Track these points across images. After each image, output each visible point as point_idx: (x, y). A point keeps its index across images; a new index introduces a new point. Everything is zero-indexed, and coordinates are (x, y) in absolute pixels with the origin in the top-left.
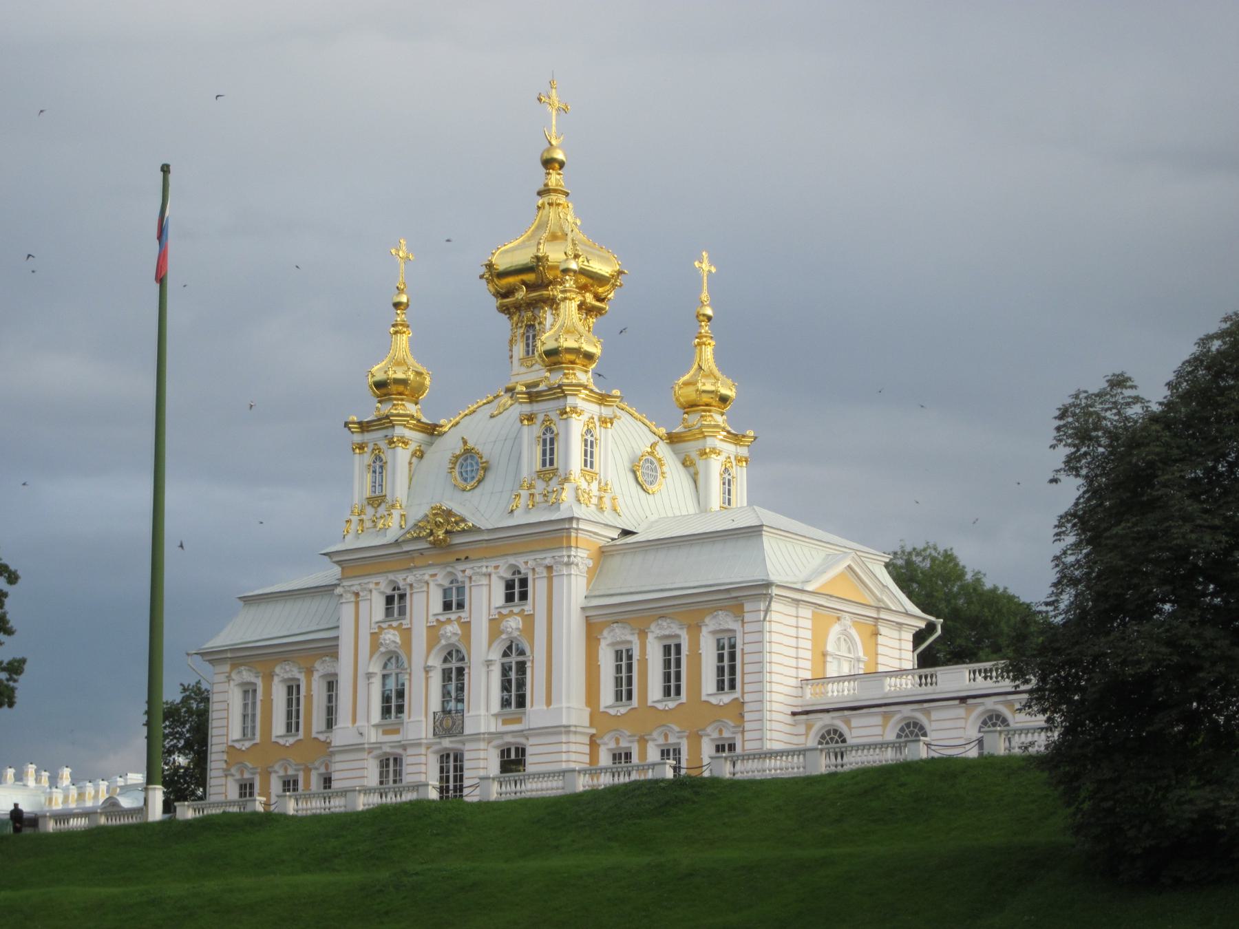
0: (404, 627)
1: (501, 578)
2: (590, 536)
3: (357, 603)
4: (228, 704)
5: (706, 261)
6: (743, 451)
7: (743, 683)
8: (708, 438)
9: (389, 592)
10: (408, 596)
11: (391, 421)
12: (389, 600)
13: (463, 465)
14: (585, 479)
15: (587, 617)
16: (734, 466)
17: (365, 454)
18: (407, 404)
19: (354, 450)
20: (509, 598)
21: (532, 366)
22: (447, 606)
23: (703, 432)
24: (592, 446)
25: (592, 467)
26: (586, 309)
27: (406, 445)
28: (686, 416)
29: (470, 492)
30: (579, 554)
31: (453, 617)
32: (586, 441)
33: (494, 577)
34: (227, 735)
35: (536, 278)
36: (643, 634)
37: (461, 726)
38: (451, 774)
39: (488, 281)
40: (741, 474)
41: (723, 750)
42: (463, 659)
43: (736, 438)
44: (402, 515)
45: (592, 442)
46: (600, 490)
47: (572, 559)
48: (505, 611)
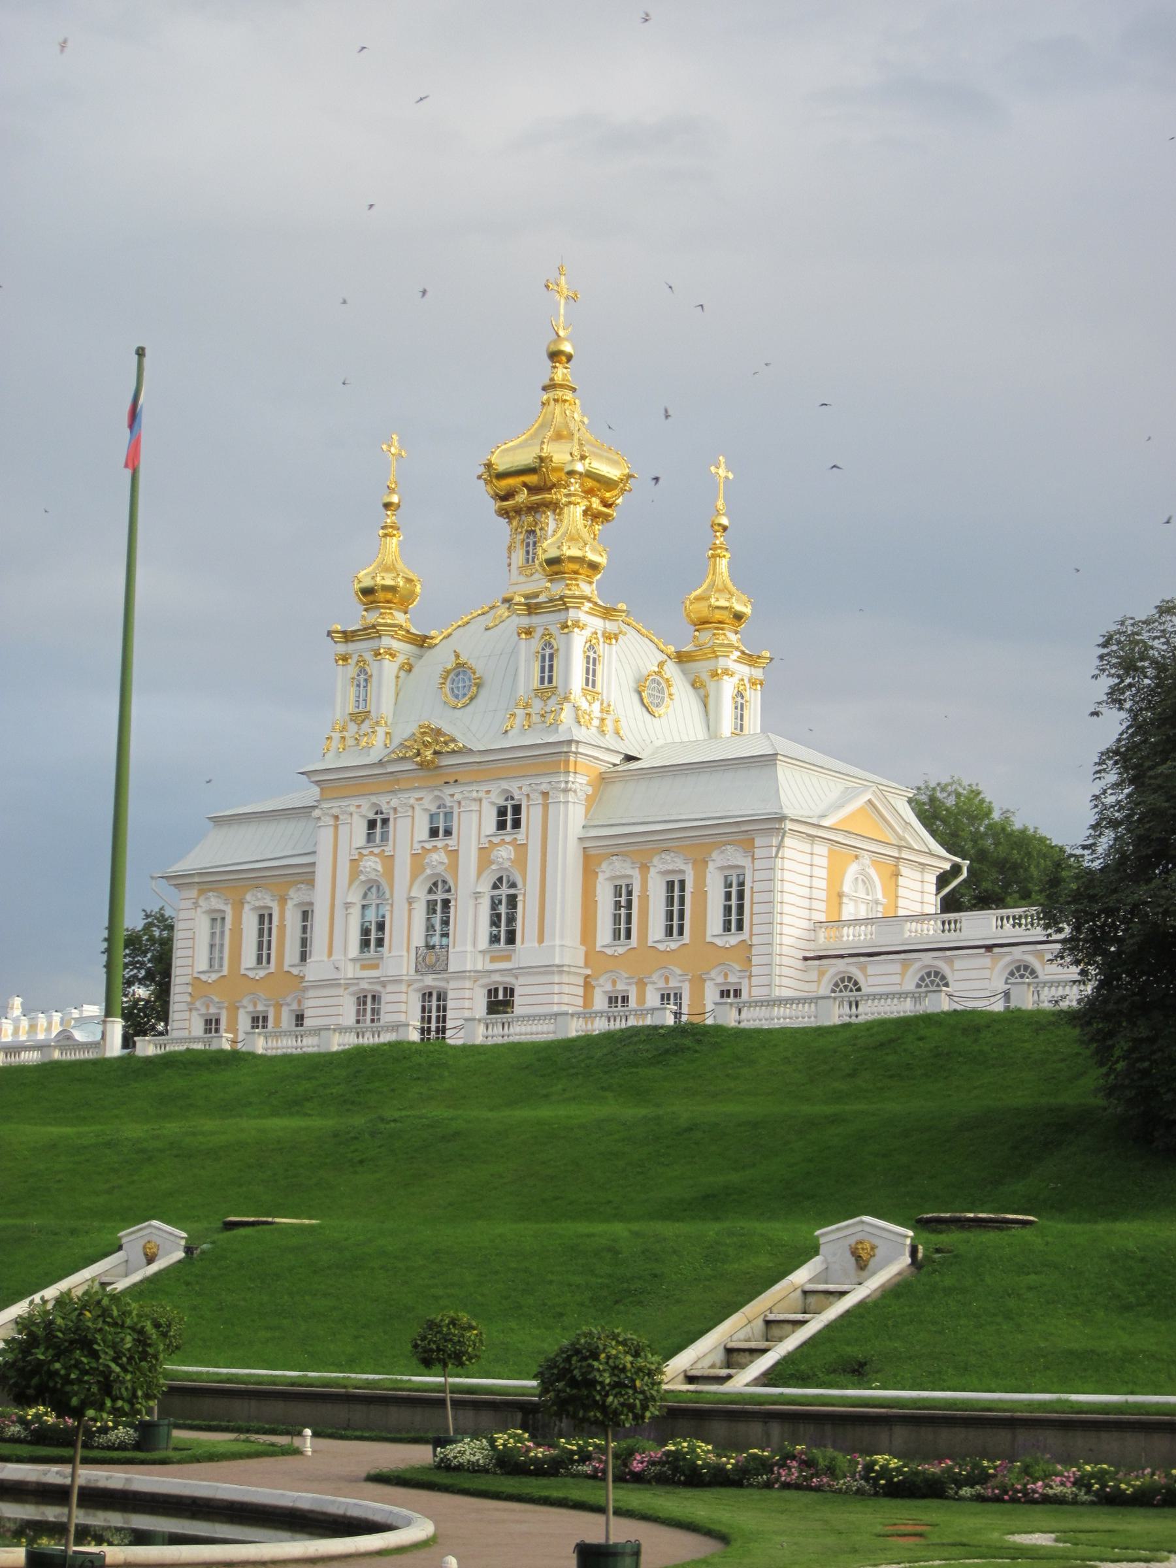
0: (387, 854)
1: (493, 803)
3: (336, 827)
5: (723, 466)
6: (758, 673)
7: (752, 925)
9: (372, 816)
10: (391, 821)
11: (378, 632)
12: (372, 824)
18: (396, 613)
19: (336, 661)
20: (501, 825)
21: (532, 575)
22: (434, 833)
23: (714, 652)
24: (594, 664)
25: (594, 686)
26: (592, 516)
28: (697, 633)
29: (463, 709)
31: (440, 844)
32: (588, 657)
33: (485, 803)
34: (192, 966)
35: (539, 480)
36: (644, 868)
38: (434, 1014)
39: (487, 482)
40: (754, 698)
41: (728, 996)
42: (449, 890)
43: (750, 659)
45: (594, 659)
46: (602, 711)
47: (570, 785)
48: (496, 840)
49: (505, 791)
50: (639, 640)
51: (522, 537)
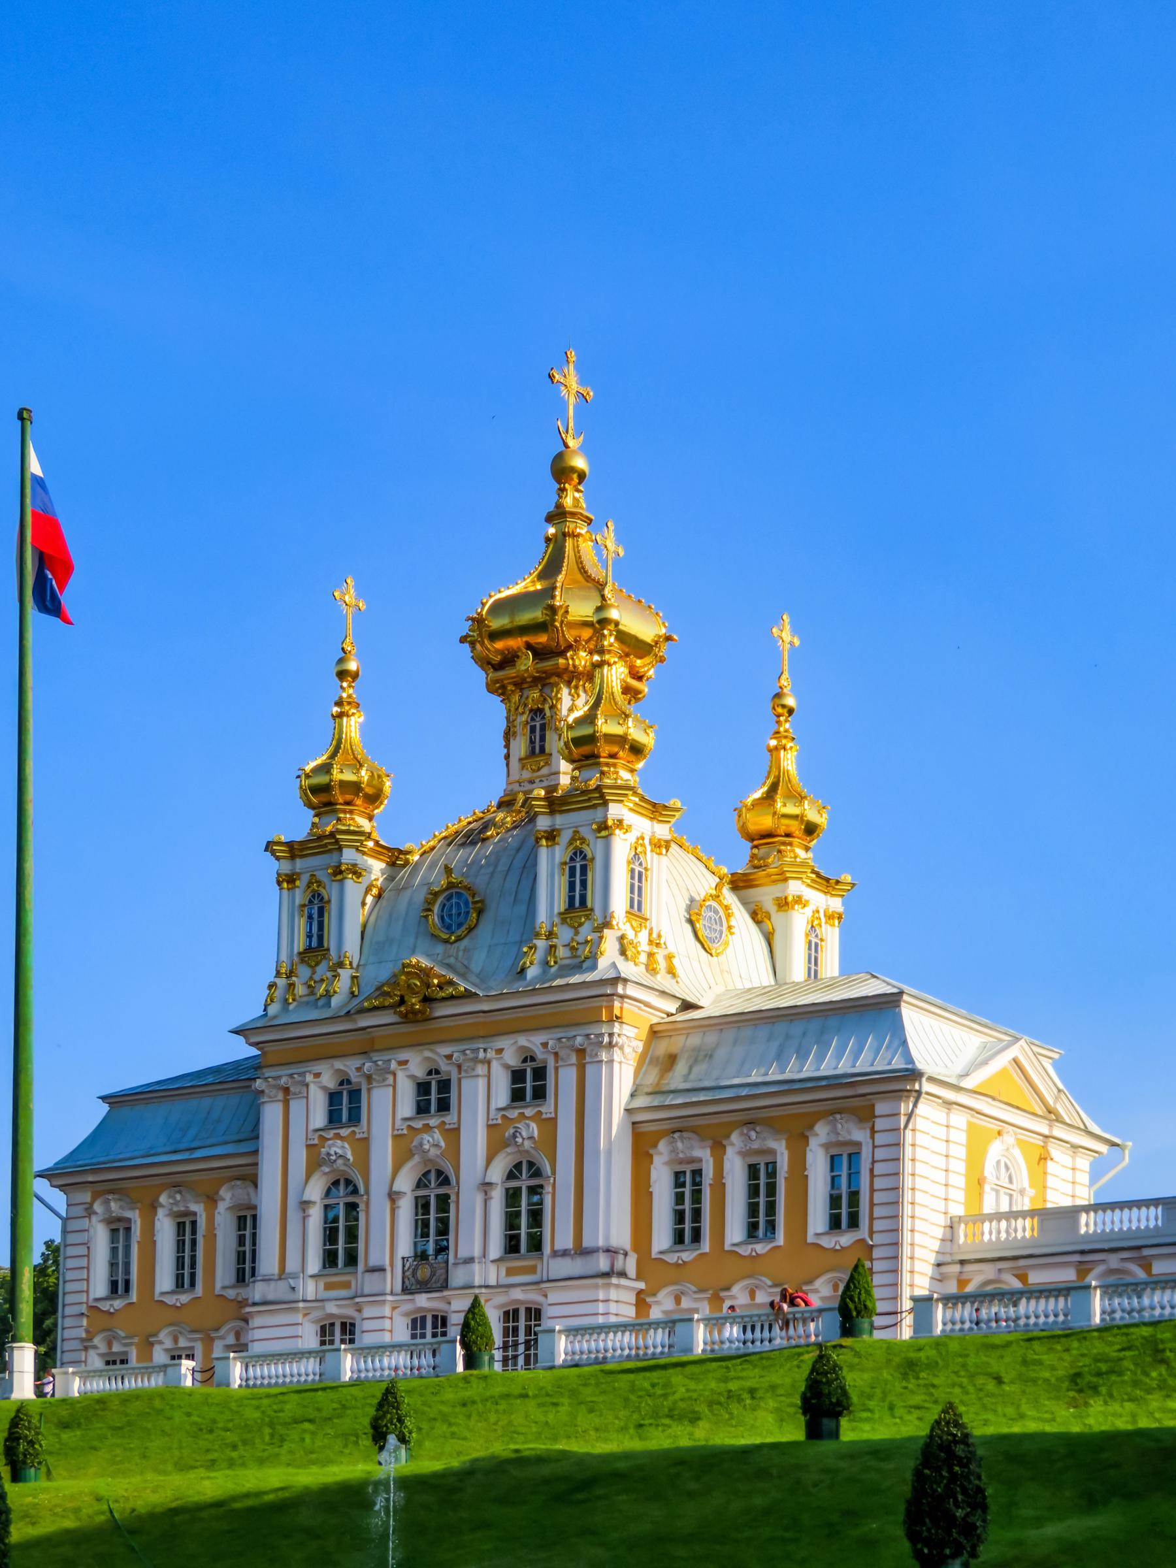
2: (639, 1008)
3: (286, 1104)
4: (88, 1248)
5: (787, 627)
6: (836, 904)
8: (791, 882)
13: (444, 905)
14: (632, 926)
15: (634, 1123)
16: (823, 924)
17: (297, 890)
19: (279, 883)
21: (539, 769)
23: (783, 873)
24: (640, 880)
27: (358, 878)
28: (755, 851)
30: (624, 1032)
31: (433, 1122)
32: (632, 871)
34: (87, 1292)
36: (719, 1148)
37: (444, 1276)
40: (832, 936)
43: (826, 883)
44: (353, 978)
45: (640, 874)
46: (651, 942)
49: (523, 1048)
50: (685, 857)
51: (524, 718)
